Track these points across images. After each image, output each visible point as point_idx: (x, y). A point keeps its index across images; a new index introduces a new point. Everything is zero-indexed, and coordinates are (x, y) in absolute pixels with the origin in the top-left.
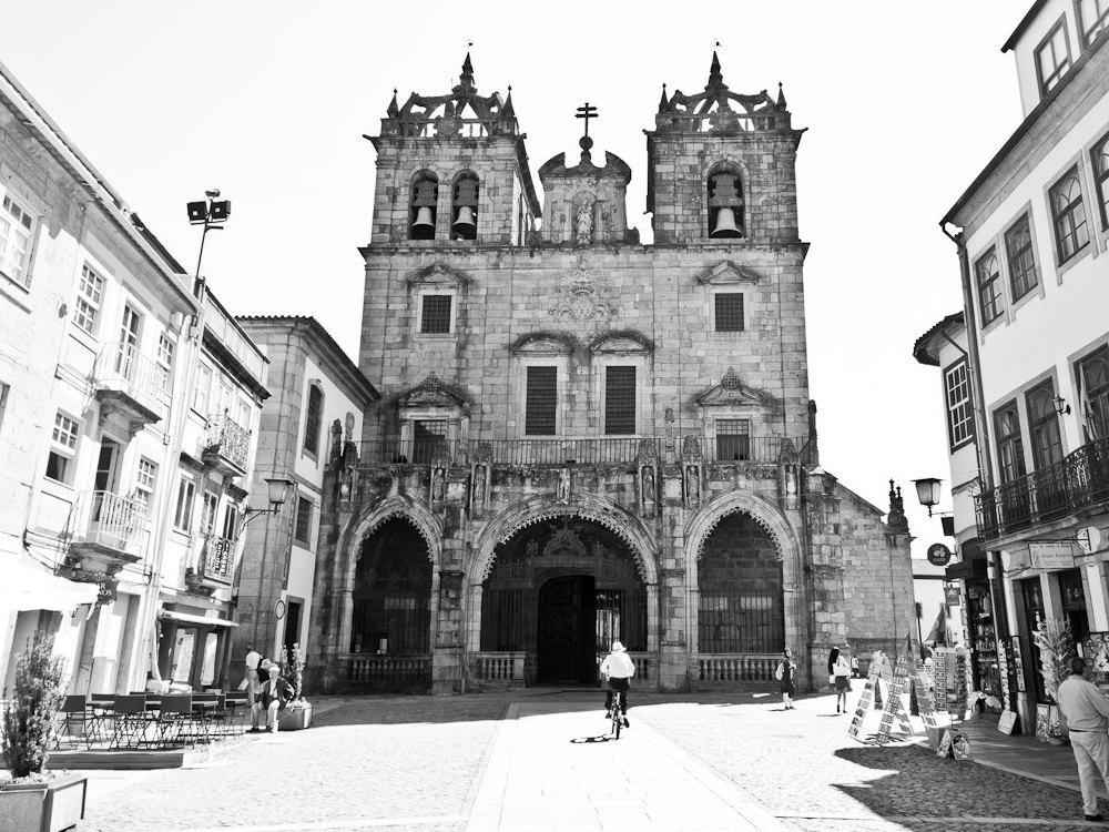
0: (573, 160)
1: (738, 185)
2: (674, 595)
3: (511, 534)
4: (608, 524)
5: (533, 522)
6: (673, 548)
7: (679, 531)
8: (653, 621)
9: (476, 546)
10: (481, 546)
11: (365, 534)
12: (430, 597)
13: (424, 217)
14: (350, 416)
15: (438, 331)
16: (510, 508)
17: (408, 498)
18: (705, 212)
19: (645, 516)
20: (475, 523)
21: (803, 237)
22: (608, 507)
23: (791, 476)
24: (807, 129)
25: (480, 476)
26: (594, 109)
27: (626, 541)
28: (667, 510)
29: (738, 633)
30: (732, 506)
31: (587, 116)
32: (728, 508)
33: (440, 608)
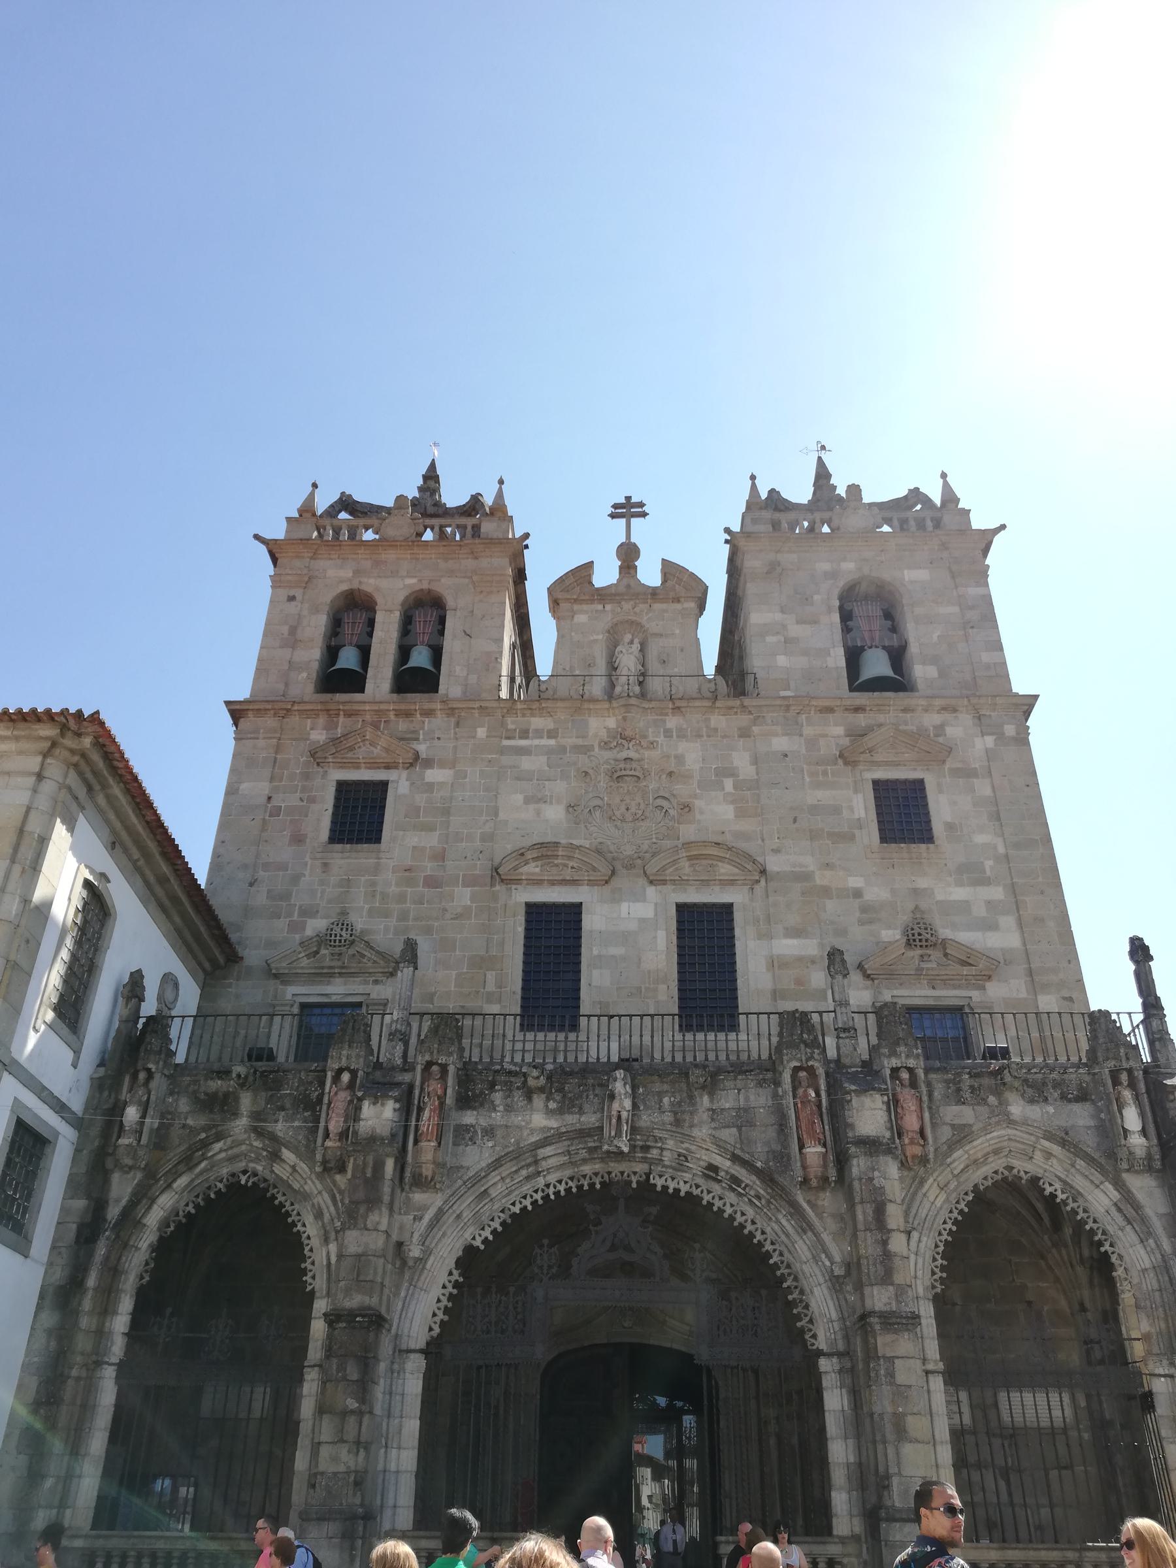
0: (606, 575)
1: (891, 617)
2: (901, 1378)
3: (496, 1224)
4: (718, 1204)
5: (546, 1198)
6: (887, 1255)
7: (894, 1216)
8: (840, 1452)
9: (415, 1252)
10: (427, 1253)
11: (165, 1223)
12: (301, 1380)
13: (348, 659)
14: (169, 981)
15: (359, 841)
16: (497, 1164)
17: (273, 1138)
18: (840, 651)
19: (805, 1182)
20: (419, 1197)
21: (1020, 685)
22: (718, 1160)
23: (1127, 1094)
24: (1003, 527)
25: (434, 1086)
26: (641, 505)
27: (760, 1245)
28: (858, 1165)
29: (1002, 1484)
30: (998, 1164)
31: (629, 516)
32: (986, 1170)
33: (322, 1410)
